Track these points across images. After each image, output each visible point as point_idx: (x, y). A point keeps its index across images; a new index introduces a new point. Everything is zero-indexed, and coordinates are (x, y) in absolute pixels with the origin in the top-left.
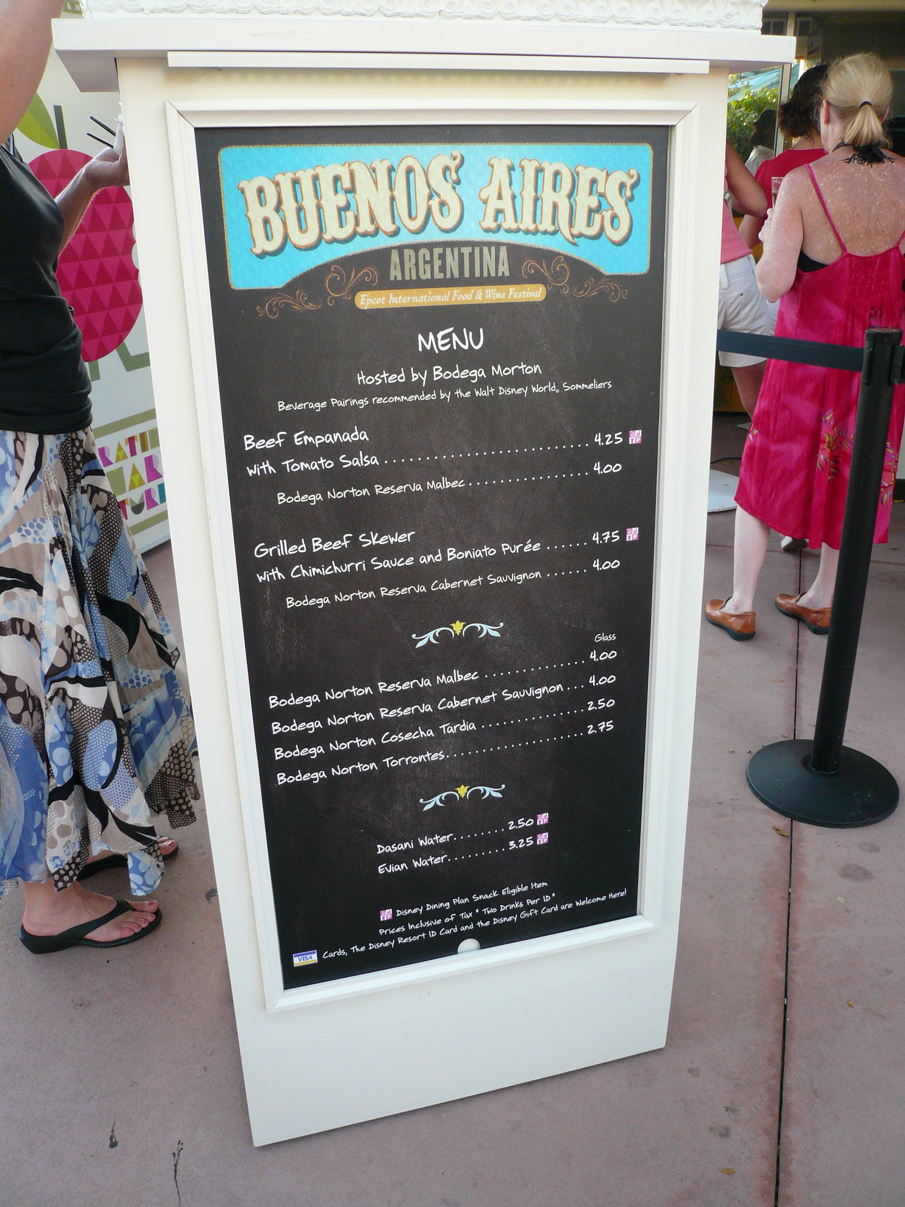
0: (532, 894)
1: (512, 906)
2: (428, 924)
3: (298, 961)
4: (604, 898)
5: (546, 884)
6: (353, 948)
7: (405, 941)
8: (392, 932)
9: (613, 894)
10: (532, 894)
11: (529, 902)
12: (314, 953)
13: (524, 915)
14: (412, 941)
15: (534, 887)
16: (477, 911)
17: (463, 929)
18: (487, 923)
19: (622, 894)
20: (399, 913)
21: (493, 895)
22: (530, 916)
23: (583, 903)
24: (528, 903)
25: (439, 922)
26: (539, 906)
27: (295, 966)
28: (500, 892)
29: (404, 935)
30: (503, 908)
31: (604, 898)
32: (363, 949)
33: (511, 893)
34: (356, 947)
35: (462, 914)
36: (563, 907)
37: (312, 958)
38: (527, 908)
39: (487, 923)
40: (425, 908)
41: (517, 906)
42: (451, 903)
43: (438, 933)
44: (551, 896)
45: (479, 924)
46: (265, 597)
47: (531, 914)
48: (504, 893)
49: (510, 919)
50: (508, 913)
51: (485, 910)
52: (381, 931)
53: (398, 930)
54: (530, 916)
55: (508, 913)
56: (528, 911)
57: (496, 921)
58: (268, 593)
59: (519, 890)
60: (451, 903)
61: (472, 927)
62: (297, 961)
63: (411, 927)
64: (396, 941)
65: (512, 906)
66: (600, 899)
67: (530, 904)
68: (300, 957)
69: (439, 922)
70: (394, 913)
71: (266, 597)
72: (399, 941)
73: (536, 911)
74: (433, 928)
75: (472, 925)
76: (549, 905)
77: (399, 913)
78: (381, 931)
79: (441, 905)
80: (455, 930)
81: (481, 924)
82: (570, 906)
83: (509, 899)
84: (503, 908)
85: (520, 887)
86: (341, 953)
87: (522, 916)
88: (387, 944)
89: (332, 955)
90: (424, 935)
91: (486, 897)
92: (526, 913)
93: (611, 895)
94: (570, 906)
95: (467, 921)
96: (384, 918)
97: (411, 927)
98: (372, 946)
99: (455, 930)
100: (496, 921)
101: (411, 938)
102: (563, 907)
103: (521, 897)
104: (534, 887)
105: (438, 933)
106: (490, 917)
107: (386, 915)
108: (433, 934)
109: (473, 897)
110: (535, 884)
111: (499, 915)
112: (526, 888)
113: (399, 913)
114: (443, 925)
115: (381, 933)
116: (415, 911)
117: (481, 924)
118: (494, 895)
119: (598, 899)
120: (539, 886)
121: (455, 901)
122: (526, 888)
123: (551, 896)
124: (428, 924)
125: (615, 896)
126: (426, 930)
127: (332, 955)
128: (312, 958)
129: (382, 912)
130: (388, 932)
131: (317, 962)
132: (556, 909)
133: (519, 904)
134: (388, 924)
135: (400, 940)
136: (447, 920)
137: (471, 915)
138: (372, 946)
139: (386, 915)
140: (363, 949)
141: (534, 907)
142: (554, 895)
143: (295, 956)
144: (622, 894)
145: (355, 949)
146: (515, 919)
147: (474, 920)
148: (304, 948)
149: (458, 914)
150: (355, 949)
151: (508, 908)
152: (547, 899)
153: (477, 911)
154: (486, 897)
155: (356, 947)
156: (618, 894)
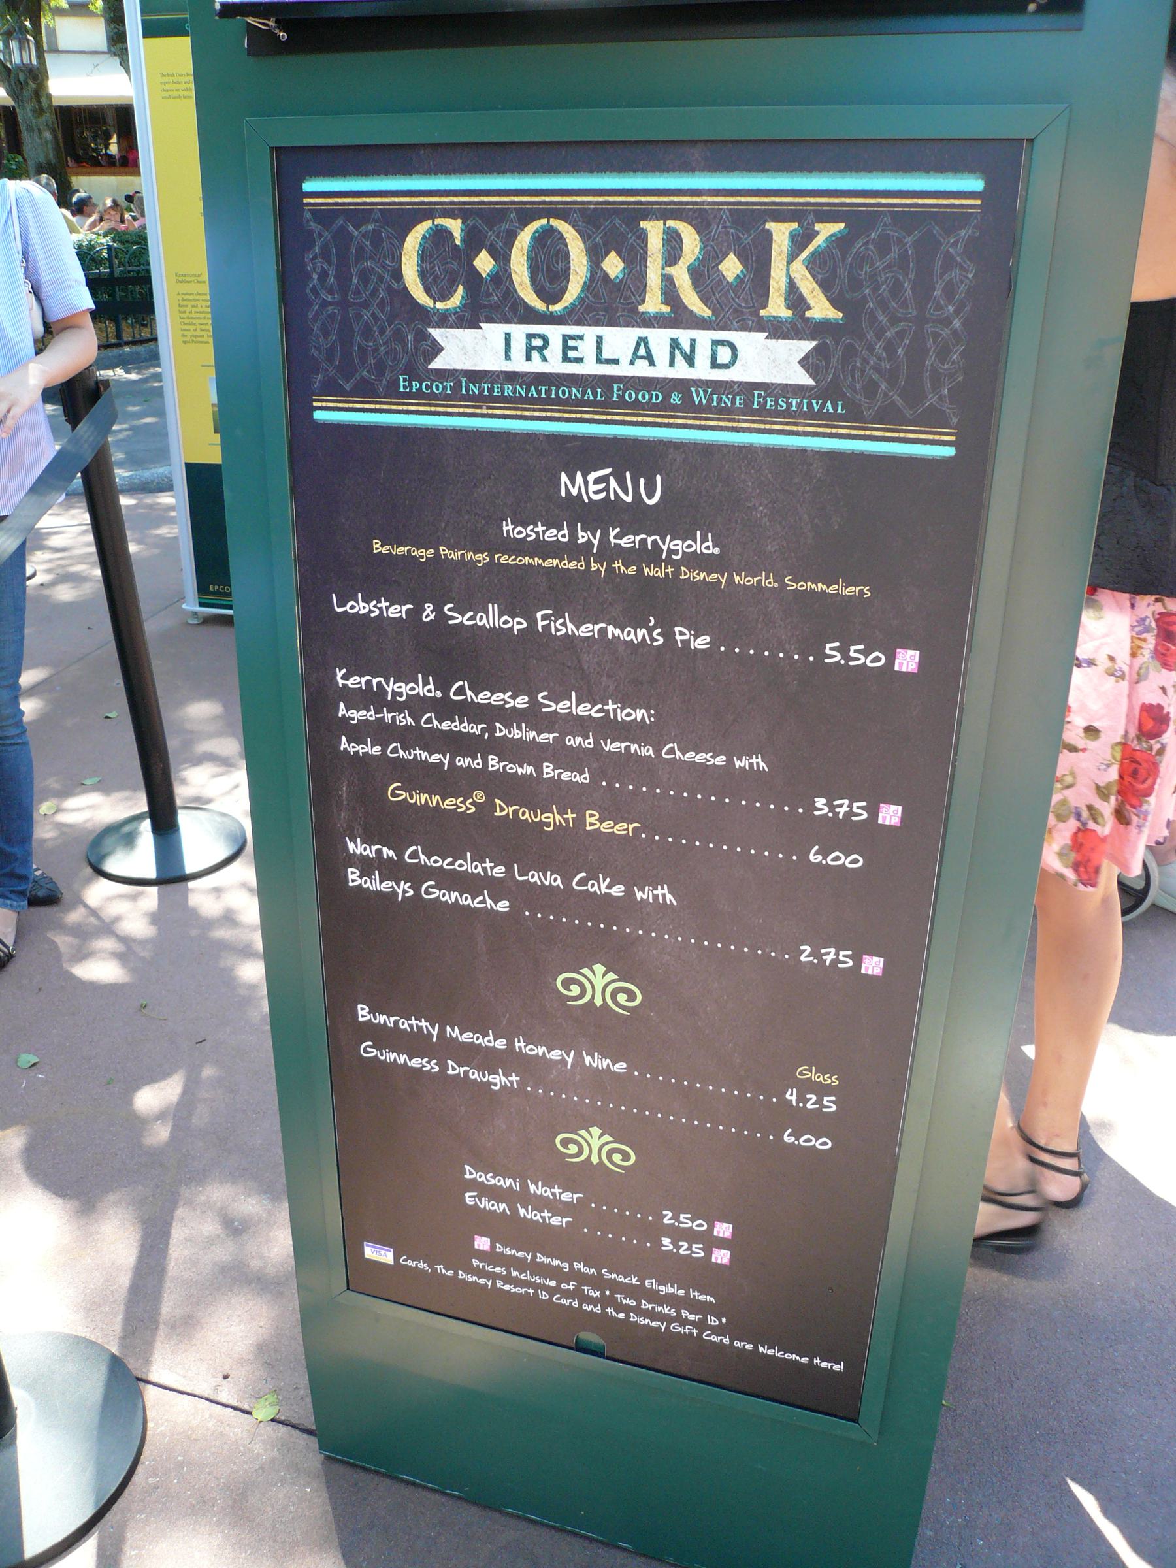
0: (695, 1306)
2: (538, 1280)
4: (805, 1360)
5: (712, 1299)
6: (438, 1267)
7: (506, 1287)
8: (489, 1268)
9: (822, 1361)
10: (695, 1306)
11: (684, 1313)
12: (390, 1251)
13: (676, 1328)
14: (515, 1292)
16: (608, 1293)
17: (585, 1307)
18: (621, 1316)
19: (836, 1368)
20: (499, 1248)
21: (631, 1280)
22: (685, 1333)
23: (770, 1352)
24: (683, 1314)
25: (553, 1283)
26: (702, 1325)
28: (642, 1280)
29: (508, 1279)
30: (645, 1305)
31: (805, 1360)
32: (450, 1273)
33: (659, 1291)
34: (442, 1267)
35: (586, 1288)
36: (737, 1344)
38: (684, 1322)
39: (621, 1316)
40: (534, 1257)
41: (666, 1312)
42: (571, 1266)
43: (551, 1296)
44: (720, 1321)
45: (609, 1310)
48: (647, 1284)
49: (655, 1324)
50: (652, 1315)
51: (619, 1296)
53: (497, 1270)
55: (652, 1315)
57: (633, 1318)
59: (671, 1290)
60: (571, 1266)
61: (598, 1310)
62: (371, 1252)
63: (515, 1274)
64: (494, 1284)
65: (660, 1308)
66: (798, 1358)
67: (686, 1317)
68: (373, 1249)
69: (553, 1283)
70: (493, 1246)
73: (695, 1331)
75: (599, 1308)
76: (716, 1331)
78: (475, 1262)
79: (558, 1262)
81: (610, 1311)
82: (749, 1347)
83: (654, 1297)
84: (645, 1305)
86: (422, 1265)
87: (674, 1328)
88: (482, 1281)
89: (412, 1264)
90: (531, 1291)
91: (621, 1279)
92: (680, 1326)
93: (817, 1361)
94: (749, 1347)
97: (515, 1274)
98: (462, 1275)
99: (575, 1304)
100: (633, 1318)
101: (515, 1288)
102: (737, 1344)
103: (670, 1300)
104: (694, 1296)
105: (551, 1296)
106: (627, 1309)
108: (544, 1296)
110: (696, 1294)
111: (638, 1311)
112: (681, 1293)
113: (499, 1248)
116: (521, 1254)
117: (610, 1311)
118: (634, 1282)
120: (702, 1298)
121: (577, 1265)
122: (681, 1293)
123: (720, 1321)
124: (538, 1280)
125: (824, 1365)
127: (412, 1264)
130: (484, 1266)
133: (669, 1310)
135: (499, 1284)
136: (564, 1286)
137: (598, 1293)
138: (462, 1275)
139: (482, 1243)
140: (450, 1273)
141: (693, 1323)
142: (724, 1320)
144: (836, 1368)
146: (663, 1327)
147: (605, 1302)
149: (580, 1284)
152: (713, 1321)
153: (608, 1293)
154: (621, 1279)
155: (442, 1267)
156: (830, 1364)
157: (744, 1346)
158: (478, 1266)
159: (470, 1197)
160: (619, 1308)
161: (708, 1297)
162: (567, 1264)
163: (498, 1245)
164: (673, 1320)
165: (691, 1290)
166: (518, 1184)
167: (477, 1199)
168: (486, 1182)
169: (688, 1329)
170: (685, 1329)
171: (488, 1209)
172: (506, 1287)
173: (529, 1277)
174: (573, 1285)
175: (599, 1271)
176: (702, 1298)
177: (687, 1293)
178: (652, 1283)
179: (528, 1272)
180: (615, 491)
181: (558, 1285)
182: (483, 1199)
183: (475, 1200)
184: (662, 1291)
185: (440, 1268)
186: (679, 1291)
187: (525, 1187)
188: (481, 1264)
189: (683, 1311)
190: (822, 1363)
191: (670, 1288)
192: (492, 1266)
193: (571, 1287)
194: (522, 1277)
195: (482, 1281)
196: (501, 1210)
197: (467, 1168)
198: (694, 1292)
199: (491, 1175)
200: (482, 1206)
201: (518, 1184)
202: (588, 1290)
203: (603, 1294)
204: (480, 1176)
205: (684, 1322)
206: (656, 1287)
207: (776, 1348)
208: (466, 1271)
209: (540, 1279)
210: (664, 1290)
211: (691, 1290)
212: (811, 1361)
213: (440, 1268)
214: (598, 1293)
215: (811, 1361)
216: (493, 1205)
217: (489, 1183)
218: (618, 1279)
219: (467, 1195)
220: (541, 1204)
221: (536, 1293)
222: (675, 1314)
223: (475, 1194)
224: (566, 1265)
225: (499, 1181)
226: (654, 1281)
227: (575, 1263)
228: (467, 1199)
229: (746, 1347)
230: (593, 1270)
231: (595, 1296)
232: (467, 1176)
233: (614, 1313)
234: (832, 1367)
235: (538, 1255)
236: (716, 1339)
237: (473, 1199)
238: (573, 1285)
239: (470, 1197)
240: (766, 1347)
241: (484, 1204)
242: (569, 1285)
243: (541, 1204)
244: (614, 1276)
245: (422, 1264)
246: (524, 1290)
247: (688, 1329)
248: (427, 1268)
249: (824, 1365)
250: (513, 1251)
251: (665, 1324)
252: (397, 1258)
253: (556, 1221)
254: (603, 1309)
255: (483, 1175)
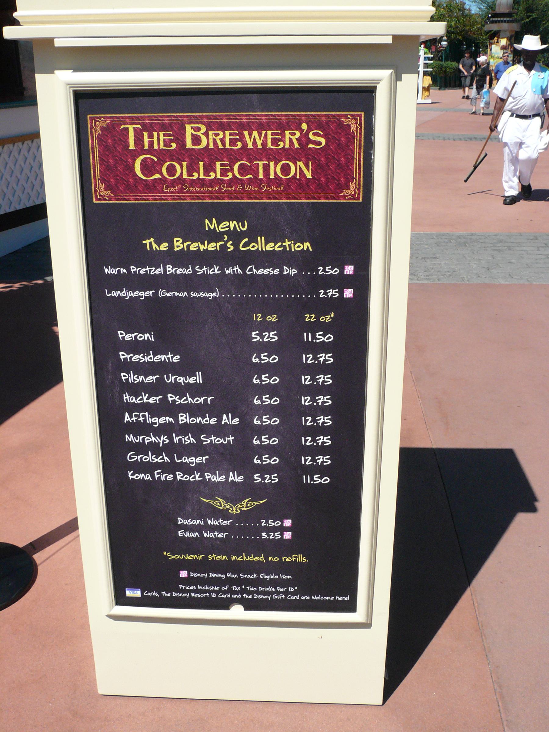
1: (267, 589)
2: (211, 588)
3: (129, 593)
4: (332, 598)
5: (290, 577)
6: (163, 593)
7: (196, 595)
8: (187, 588)
11: (278, 589)
12: (139, 590)
13: (275, 597)
15: (282, 577)
16: (243, 587)
17: (234, 596)
18: (250, 597)
19: (346, 599)
20: (192, 575)
21: (254, 576)
22: (279, 598)
23: (317, 598)
24: (278, 589)
25: (218, 588)
27: (127, 596)
29: (196, 591)
30: (261, 589)
31: (332, 598)
32: (169, 595)
33: (267, 578)
34: (165, 592)
35: (233, 587)
36: (303, 598)
37: (137, 593)
38: (278, 593)
39: (250, 597)
40: (209, 575)
41: (270, 590)
42: (226, 576)
45: (244, 595)
46: (108, 367)
47: (280, 597)
48: (261, 577)
49: (266, 597)
50: (264, 593)
51: (248, 587)
52: (181, 586)
53: (191, 588)
54: (279, 598)
55: (264, 593)
56: (278, 595)
57: (256, 596)
58: (110, 365)
59: (272, 577)
60: (226, 576)
61: (239, 596)
62: (129, 593)
63: (200, 588)
64: (190, 595)
65: (267, 589)
66: (329, 598)
67: (279, 590)
68: (130, 591)
69: (218, 588)
70: (189, 574)
71: (109, 368)
72: (192, 595)
73: (284, 596)
74: (214, 591)
75: (240, 595)
76: (293, 594)
77: (192, 575)
78: (181, 586)
79: (219, 575)
80: (229, 596)
81: (245, 596)
82: (308, 598)
83: (265, 583)
84: (261, 589)
85: (272, 575)
86: (155, 594)
87: (274, 597)
88: (184, 595)
89: (150, 594)
90: (208, 595)
91: (249, 576)
93: (337, 598)
94: (308, 598)
95: (236, 593)
96: (182, 575)
97: (200, 588)
98: (174, 594)
99: (229, 596)
100: (256, 596)
101: (200, 595)
102: (303, 598)
104: (282, 577)
106: (252, 593)
107: (184, 574)
108: (214, 595)
109: (240, 575)
110: (283, 576)
112: (276, 577)
113: (192, 575)
114: (220, 591)
115: (180, 587)
116: (202, 575)
117: (245, 596)
118: (255, 577)
119: (328, 598)
120: (286, 577)
122: (276, 577)
124: (211, 588)
125: (340, 599)
126: (210, 592)
127: (150, 594)
128: (137, 593)
129: (181, 572)
130: (185, 587)
131: (140, 596)
132: (298, 597)
133: (272, 589)
134: (186, 581)
136: (223, 588)
137: (239, 588)
138: (174, 594)
139: (184, 574)
140: (169, 595)
143: (127, 590)
144: (346, 599)
145: (164, 593)
146: (270, 598)
147: (242, 592)
148: (133, 586)
149: (231, 586)
150: (164, 593)
151: (264, 589)
152: (291, 589)
153: (243, 587)
154: (249, 576)
156: (343, 598)
157: (306, 598)
158: (182, 588)
159: (180, 533)
160: (249, 593)
161: (289, 576)
162: (224, 575)
163: (191, 573)
164: (274, 593)
165: (281, 575)
166: (203, 521)
167: (184, 533)
168: (188, 524)
169: (281, 596)
170: (279, 596)
171: (189, 537)
172: (196, 595)
173: (207, 588)
174: (227, 587)
175: (239, 575)
176: (286, 577)
177: (279, 577)
178: (263, 575)
179: (206, 585)
180: (208, 224)
181: (220, 588)
182: (187, 532)
183: (183, 534)
184: (268, 578)
185: (164, 593)
186: (276, 577)
187: (206, 522)
188: (184, 587)
189: (278, 588)
190: (340, 598)
191: (271, 576)
192: (189, 587)
193: (227, 588)
194: (203, 588)
195: (184, 595)
196: (196, 536)
197: (179, 519)
198: (282, 575)
199: (190, 520)
200: (186, 536)
201: (203, 521)
202: (234, 588)
203: (241, 588)
204: (185, 522)
205: (278, 593)
206: (265, 577)
207: (320, 595)
208: (176, 592)
209: (211, 587)
210: (268, 577)
211: (281, 575)
212: (335, 598)
213: (164, 593)
214: (239, 588)
215: (335, 598)
216: (191, 534)
217: (189, 524)
218: (248, 577)
219: (179, 532)
220: (213, 529)
221: (210, 595)
222: (274, 590)
223: (183, 531)
224: (224, 576)
225: (194, 522)
226: (264, 574)
227: (227, 574)
228: (179, 534)
229: (307, 599)
230: (236, 575)
231: (238, 590)
232: (179, 523)
233: (247, 596)
234: (344, 599)
235: (210, 574)
236: (293, 598)
237: (182, 533)
238: (227, 587)
239: (180, 533)
240: (315, 596)
241: (188, 535)
242: (225, 587)
243: (213, 529)
244: (246, 576)
245: (155, 593)
246: (204, 595)
247: (281, 596)
248: (158, 595)
249: (340, 599)
250: (198, 575)
251: (270, 596)
252: (142, 593)
253: (220, 536)
254: (242, 595)
255: (187, 521)
